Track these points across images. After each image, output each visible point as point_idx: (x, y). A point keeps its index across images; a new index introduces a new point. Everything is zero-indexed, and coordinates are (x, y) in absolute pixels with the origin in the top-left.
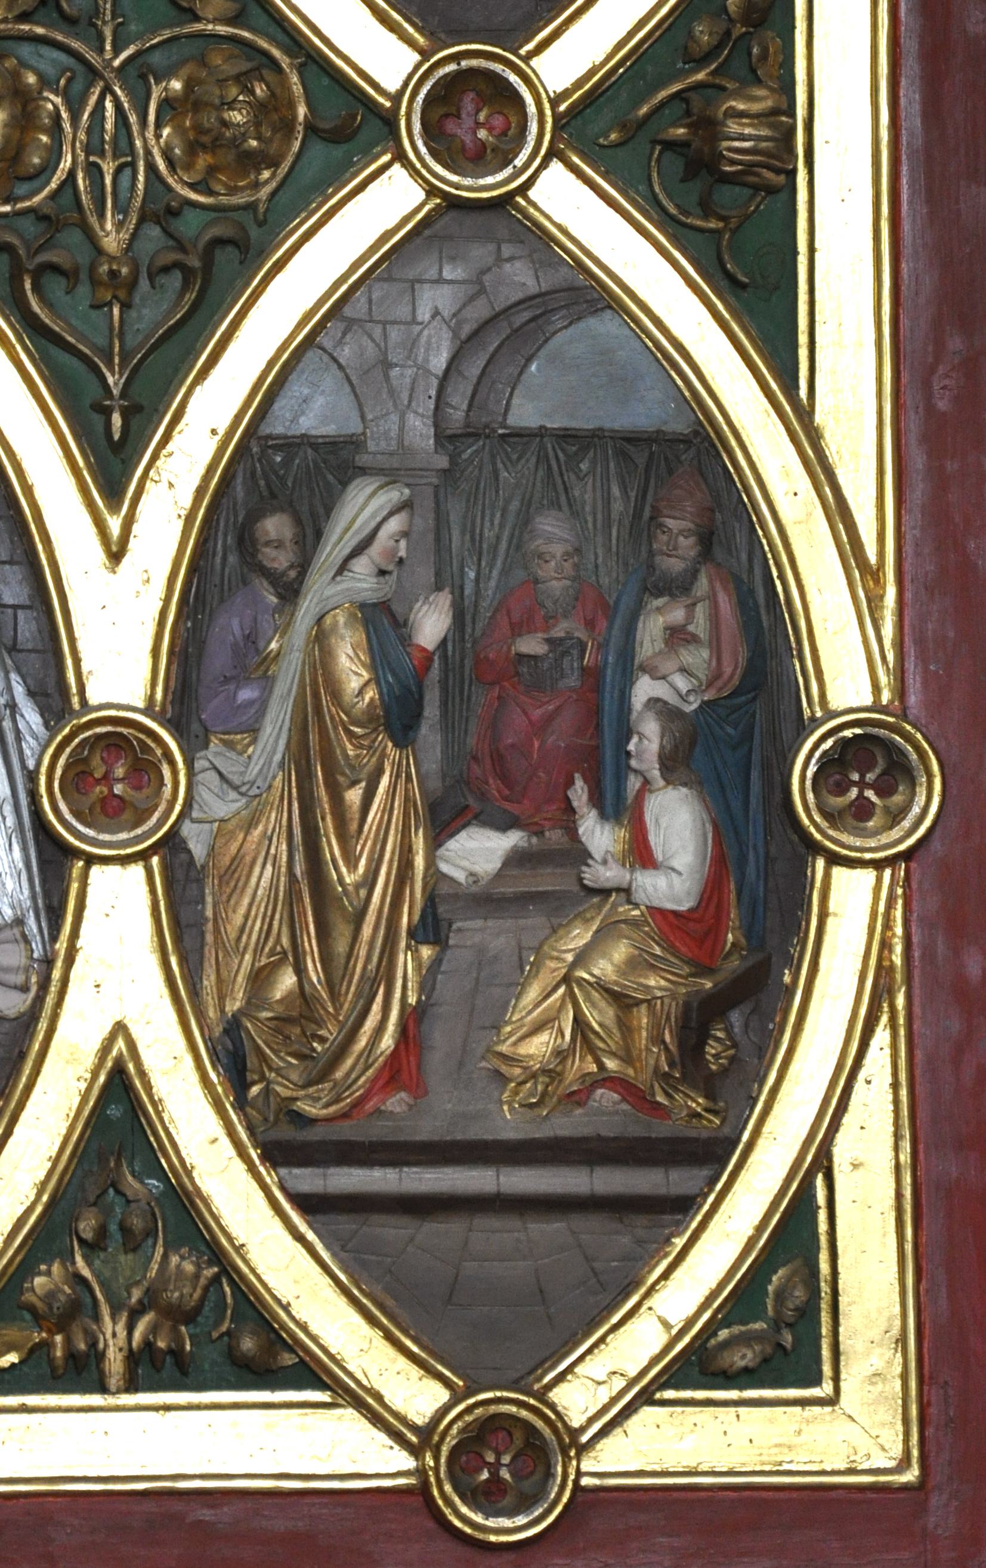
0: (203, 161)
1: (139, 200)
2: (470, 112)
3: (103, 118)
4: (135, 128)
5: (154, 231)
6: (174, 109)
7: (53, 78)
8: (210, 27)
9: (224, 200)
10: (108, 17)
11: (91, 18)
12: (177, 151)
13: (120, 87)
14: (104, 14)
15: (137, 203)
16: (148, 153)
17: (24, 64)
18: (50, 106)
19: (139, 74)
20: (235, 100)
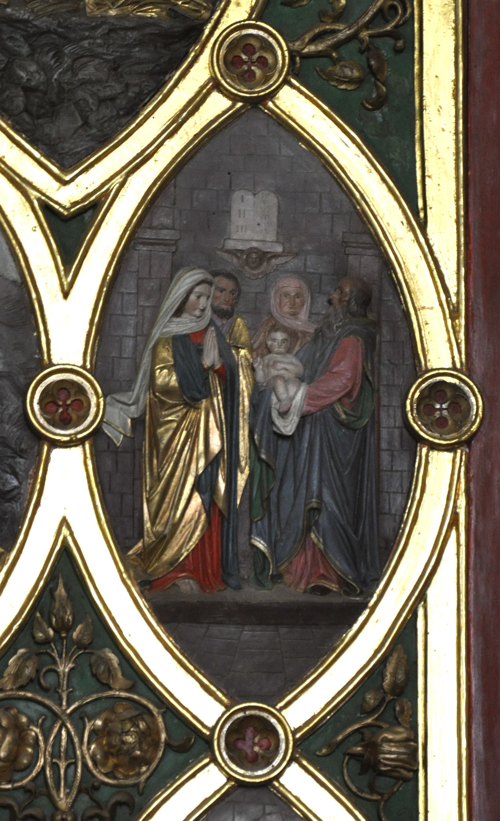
0: (112, 761)
1: (78, 781)
2: (250, 738)
3: (60, 740)
4: (77, 745)
5: (85, 798)
6: (97, 734)
7: (35, 719)
8: (117, 693)
9: (122, 782)
10: (65, 688)
11: (56, 689)
12: (98, 757)
13: (70, 724)
14: (63, 687)
15: (77, 783)
16: (83, 757)
17: (20, 712)
18: (33, 734)
19: (80, 717)
20: (129, 731)
